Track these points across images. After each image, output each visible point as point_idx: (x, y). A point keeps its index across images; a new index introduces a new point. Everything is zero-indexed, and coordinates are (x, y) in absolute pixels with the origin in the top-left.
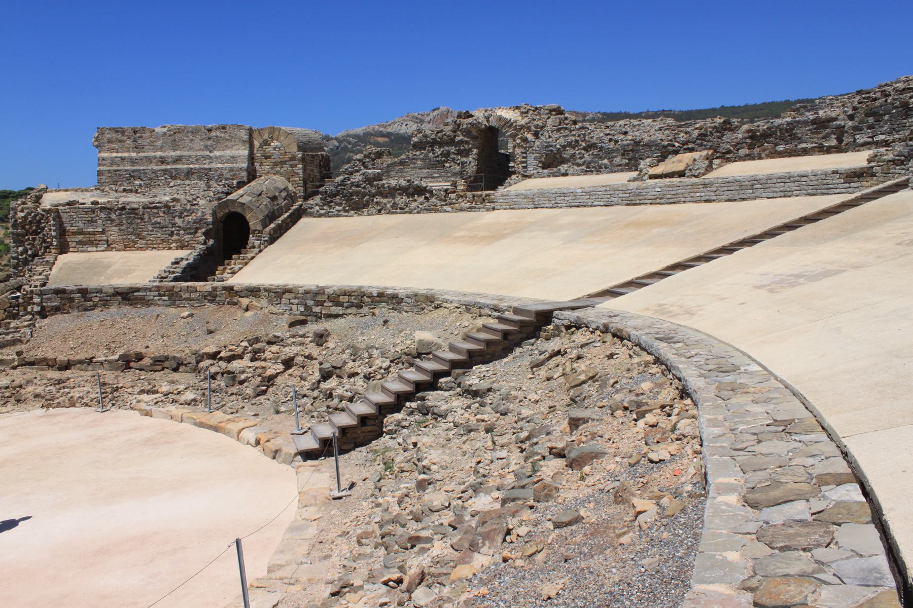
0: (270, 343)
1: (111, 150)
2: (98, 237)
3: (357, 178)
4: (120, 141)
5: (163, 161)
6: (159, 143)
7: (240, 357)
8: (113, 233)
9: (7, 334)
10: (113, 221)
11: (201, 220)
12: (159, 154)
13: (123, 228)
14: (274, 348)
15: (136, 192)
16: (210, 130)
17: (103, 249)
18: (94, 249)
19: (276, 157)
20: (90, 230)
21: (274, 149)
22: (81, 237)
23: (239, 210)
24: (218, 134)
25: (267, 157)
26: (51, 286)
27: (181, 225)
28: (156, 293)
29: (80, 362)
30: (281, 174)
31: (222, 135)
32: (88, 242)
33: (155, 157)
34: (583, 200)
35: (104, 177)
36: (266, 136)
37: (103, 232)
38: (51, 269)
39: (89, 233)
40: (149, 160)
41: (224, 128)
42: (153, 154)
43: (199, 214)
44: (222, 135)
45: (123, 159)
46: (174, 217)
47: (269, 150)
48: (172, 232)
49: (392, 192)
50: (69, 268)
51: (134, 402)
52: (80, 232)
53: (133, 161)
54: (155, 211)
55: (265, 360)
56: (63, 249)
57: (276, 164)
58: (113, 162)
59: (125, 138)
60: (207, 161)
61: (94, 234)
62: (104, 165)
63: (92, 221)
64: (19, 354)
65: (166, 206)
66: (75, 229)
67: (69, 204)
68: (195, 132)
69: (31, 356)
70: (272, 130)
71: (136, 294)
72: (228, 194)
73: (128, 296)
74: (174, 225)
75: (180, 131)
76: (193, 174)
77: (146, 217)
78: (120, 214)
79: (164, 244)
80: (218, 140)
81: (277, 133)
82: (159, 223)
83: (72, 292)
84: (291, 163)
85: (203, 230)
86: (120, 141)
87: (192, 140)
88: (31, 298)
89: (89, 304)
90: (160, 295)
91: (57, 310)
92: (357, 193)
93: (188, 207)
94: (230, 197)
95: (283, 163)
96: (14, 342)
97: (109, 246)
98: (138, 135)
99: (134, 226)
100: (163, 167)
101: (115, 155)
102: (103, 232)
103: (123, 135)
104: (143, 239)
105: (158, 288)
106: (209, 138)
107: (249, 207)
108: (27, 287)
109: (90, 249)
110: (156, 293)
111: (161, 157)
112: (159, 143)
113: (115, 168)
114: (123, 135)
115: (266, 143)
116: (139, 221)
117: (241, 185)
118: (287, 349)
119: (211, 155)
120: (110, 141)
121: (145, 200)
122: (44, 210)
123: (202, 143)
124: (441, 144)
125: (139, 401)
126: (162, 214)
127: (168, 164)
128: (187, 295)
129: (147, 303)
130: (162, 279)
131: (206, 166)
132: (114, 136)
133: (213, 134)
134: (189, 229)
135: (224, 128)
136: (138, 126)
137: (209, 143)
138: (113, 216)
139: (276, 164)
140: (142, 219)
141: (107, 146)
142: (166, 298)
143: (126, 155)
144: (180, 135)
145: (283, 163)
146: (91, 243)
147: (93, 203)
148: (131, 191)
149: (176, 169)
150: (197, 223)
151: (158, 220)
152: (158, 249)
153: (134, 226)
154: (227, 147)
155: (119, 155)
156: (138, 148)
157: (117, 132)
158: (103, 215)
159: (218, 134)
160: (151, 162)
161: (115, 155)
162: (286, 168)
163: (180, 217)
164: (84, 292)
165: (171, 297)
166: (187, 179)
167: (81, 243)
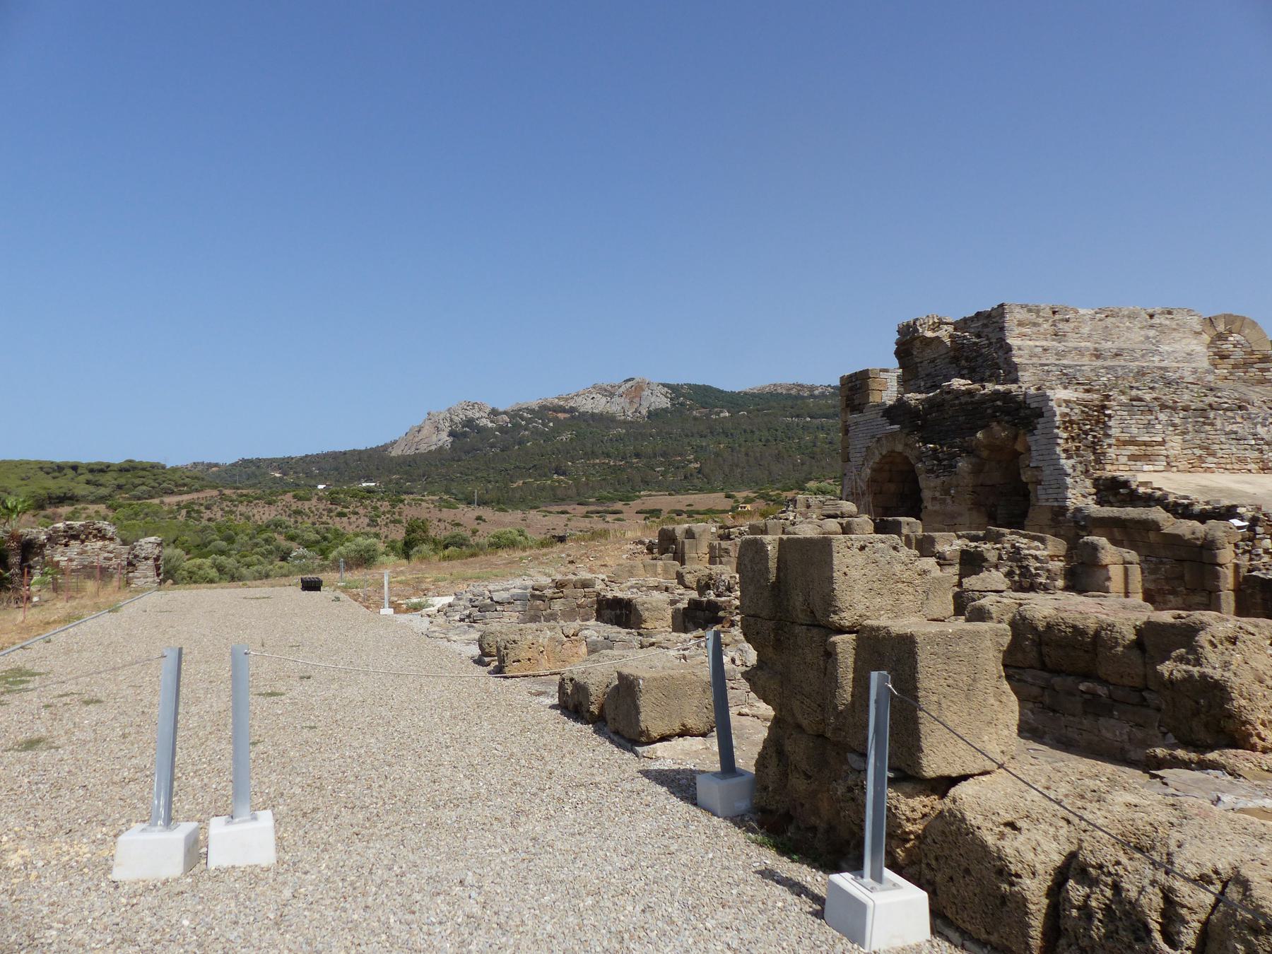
4: (1035, 324)
6: (1085, 330)
8: (1175, 444)
10: (1174, 425)
13: (1188, 437)
17: (1161, 468)
18: (1151, 468)
19: (1238, 355)
20: (1147, 439)
22: (1132, 449)
25: (1223, 357)
31: (1168, 322)
33: (1087, 349)
36: (1221, 328)
37: (1163, 443)
39: (1145, 444)
40: (1080, 352)
44: (1168, 322)
46: (1255, 424)
47: (1228, 346)
54: (1229, 414)
57: (1235, 366)
60: (1156, 358)
63: (1149, 425)
66: (1125, 437)
68: (1132, 316)
70: (1230, 319)
76: (1144, 374)
77: (1218, 422)
80: (1162, 329)
81: (1238, 324)
82: (1236, 433)
84: (1262, 365)
86: (1035, 324)
87: (1128, 328)
98: (1057, 317)
100: (1099, 363)
102: (1163, 443)
103: (1038, 316)
104: (1214, 455)
106: (1152, 326)
109: (1146, 468)
111: (1096, 349)
113: (1035, 360)
114: (1038, 316)
115: (1221, 337)
116: (1208, 428)
120: (1020, 324)
126: (1239, 420)
127: (1105, 359)
131: (1157, 364)
133: (1156, 320)
135: (1170, 313)
136: (1058, 305)
137: (1152, 333)
138: (1177, 421)
143: (1045, 343)
145: (1246, 365)
149: (1123, 367)
152: (1232, 471)
153: (1203, 435)
157: (1030, 311)
158: (1162, 417)
160: (1083, 355)
162: (1253, 372)
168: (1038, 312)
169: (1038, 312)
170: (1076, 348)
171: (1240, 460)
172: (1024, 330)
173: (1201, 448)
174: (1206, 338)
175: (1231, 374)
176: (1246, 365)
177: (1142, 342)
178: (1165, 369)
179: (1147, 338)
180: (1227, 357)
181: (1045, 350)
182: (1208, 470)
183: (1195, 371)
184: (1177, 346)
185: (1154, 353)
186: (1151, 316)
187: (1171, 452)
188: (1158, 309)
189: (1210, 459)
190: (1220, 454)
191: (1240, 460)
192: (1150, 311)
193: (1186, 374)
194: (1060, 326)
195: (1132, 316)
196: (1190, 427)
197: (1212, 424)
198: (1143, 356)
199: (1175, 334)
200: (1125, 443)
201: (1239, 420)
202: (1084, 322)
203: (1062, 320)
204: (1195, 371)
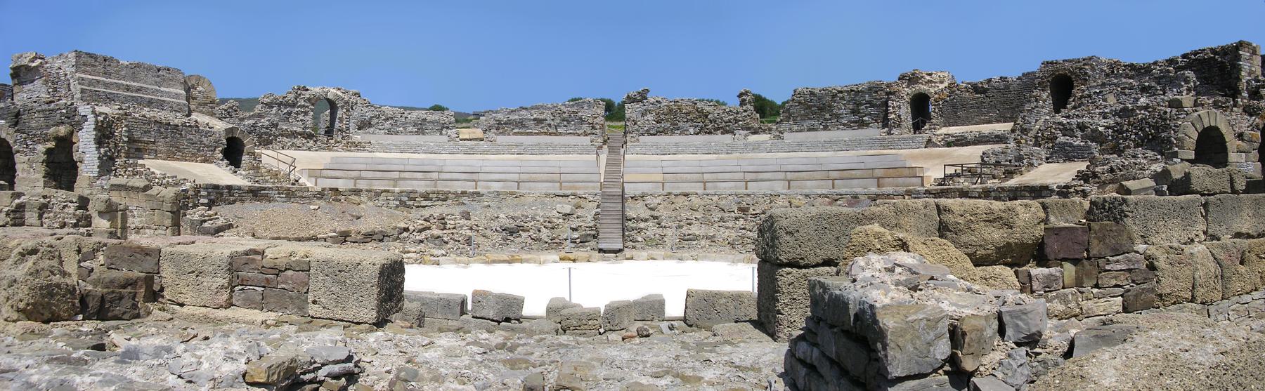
1: (85, 72)
3: (264, 122)
5: (128, 89)
8: (161, 145)
34: (435, 149)
45: (98, 82)
49: (294, 135)
53: (107, 85)
58: (90, 83)
70: (199, 78)
92: (266, 134)
95: (205, 104)
97: (156, 158)
112: (123, 73)
120: (85, 64)
124: (286, 106)
129: (269, 199)
141: (83, 68)
145: (205, 104)
154: (169, 86)
164: (229, 188)
165: (287, 195)
171: (193, 155)
182: (178, 160)
204: (179, 104)
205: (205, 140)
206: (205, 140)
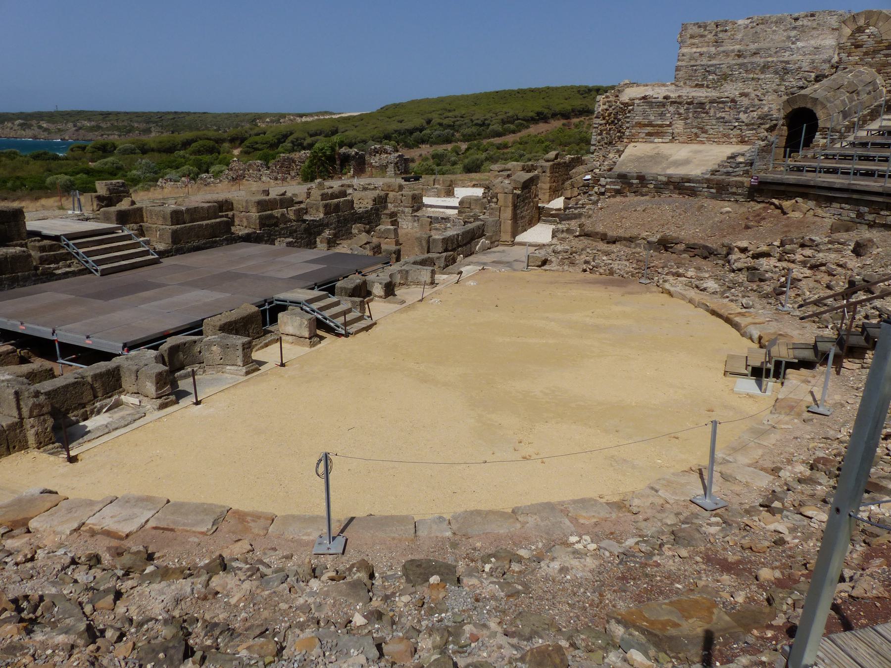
0: (803, 246)
2: (665, 129)
4: (702, 36)
6: (739, 36)
7: (766, 255)
9: (576, 209)
10: (680, 114)
11: (767, 116)
12: (737, 47)
13: (688, 121)
14: (808, 252)
15: (708, 87)
16: (796, 19)
18: (660, 140)
19: (870, 43)
20: (659, 122)
21: (869, 36)
22: (649, 129)
23: (809, 106)
24: (805, 22)
26: (617, 170)
27: (746, 121)
28: (705, 186)
29: (625, 239)
30: (871, 66)
31: (809, 23)
32: (656, 132)
33: (733, 51)
35: (681, 73)
36: (861, 22)
37: (670, 125)
38: (620, 156)
40: (727, 54)
41: (812, 15)
42: (732, 48)
43: (766, 109)
46: (739, 112)
48: (735, 127)
50: (635, 154)
51: (661, 281)
52: (650, 124)
53: (711, 57)
54: (721, 105)
55: (793, 262)
56: (632, 139)
57: (866, 54)
59: (706, 33)
60: (787, 54)
61: (661, 126)
62: (683, 60)
63: (662, 115)
64: (580, 226)
65: (733, 101)
66: (646, 122)
67: (644, 98)
68: (779, 22)
69: (589, 228)
70: (869, 15)
71: (687, 184)
72: (802, 88)
73: (681, 186)
74: (737, 120)
75: (764, 22)
76: (769, 67)
77: (712, 112)
78: (688, 109)
79: (725, 139)
81: (875, 18)
82: (723, 118)
83: (632, 178)
85: (767, 126)
86: (702, 36)
87: (774, 31)
88: (599, 180)
89: (645, 190)
90: (708, 187)
91: (618, 192)
93: (757, 102)
94: (803, 92)
96: (579, 216)
97: (673, 139)
99: (698, 117)
100: (741, 61)
101: (694, 50)
102: (670, 125)
104: (705, 132)
105: (708, 181)
106: (795, 28)
107: (822, 103)
108: (597, 171)
109: (656, 140)
110: (705, 186)
111: (739, 51)
113: (693, 63)
115: (860, 30)
116: (704, 115)
117: (818, 79)
118: (821, 255)
119: (793, 46)
120: (692, 37)
121: (714, 94)
122: (622, 104)
123: (785, 34)
125: (665, 281)
126: (727, 109)
128: (734, 190)
129: (693, 193)
130: (714, 172)
132: (696, 30)
133: (800, 23)
134: (753, 124)
135: (812, 15)
136: (721, 20)
137: (793, 33)
138: (682, 111)
139: (866, 54)
140: (707, 113)
141: (689, 41)
142: (713, 191)
143: (704, 49)
144: (761, 26)
145: (875, 52)
146: (658, 134)
147: (665, 98)
148: (702, 86)
149: (752, 63)
150: (763, 119)
151: (723, 115)
152: (718, 143)
153: (699, 120)
155: (699, 50)
156: (717, 43)
157: (700, 27)
158: (672, 109)
159: (805, 22)
161: (694, 50)
163: (745, 112)
164: (642, 178)
166: (762, 73)
167: (649, 134)
168: (705, 27)
169: (705, 27)
170: (724, 52)
171: (724, 135)
172: (696, 41)
173: (699, 128)
174: (847, 31)
175: (861, 59)
176: (875, 52)
177: (784, 41)
178: (787, 62)
179: (789, 37)
180: (861, 46)
181: (701, 54)
183: (813, 62)
184: (813, 42)
185: (785, 49)
186: (796, 19)
187: (676, 131)
188: (802, 13)
189: (703, 135)
190: (711, 132)
191: (724, 135)
192: (796, 15)
193: (804, 64)
194: (720, 35)
195: (779, 22)
196: (691, 115)
197: (707, 113)
198: (776, 53)
199: (815, 33)
200: (645, 125)
201: (727, 109)
202: (739, 30)
203: (722, 31)
205: (743, 116)
206: (743, 116)
